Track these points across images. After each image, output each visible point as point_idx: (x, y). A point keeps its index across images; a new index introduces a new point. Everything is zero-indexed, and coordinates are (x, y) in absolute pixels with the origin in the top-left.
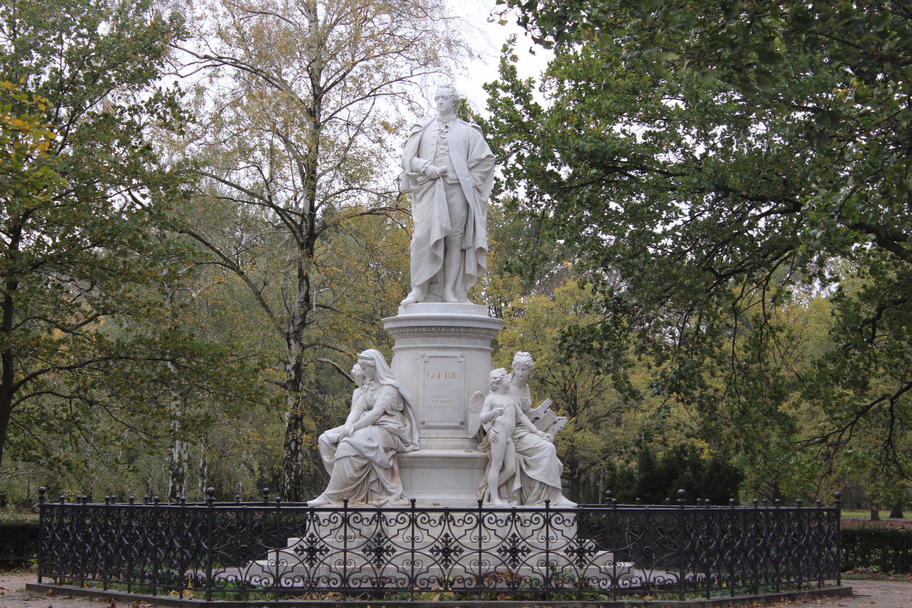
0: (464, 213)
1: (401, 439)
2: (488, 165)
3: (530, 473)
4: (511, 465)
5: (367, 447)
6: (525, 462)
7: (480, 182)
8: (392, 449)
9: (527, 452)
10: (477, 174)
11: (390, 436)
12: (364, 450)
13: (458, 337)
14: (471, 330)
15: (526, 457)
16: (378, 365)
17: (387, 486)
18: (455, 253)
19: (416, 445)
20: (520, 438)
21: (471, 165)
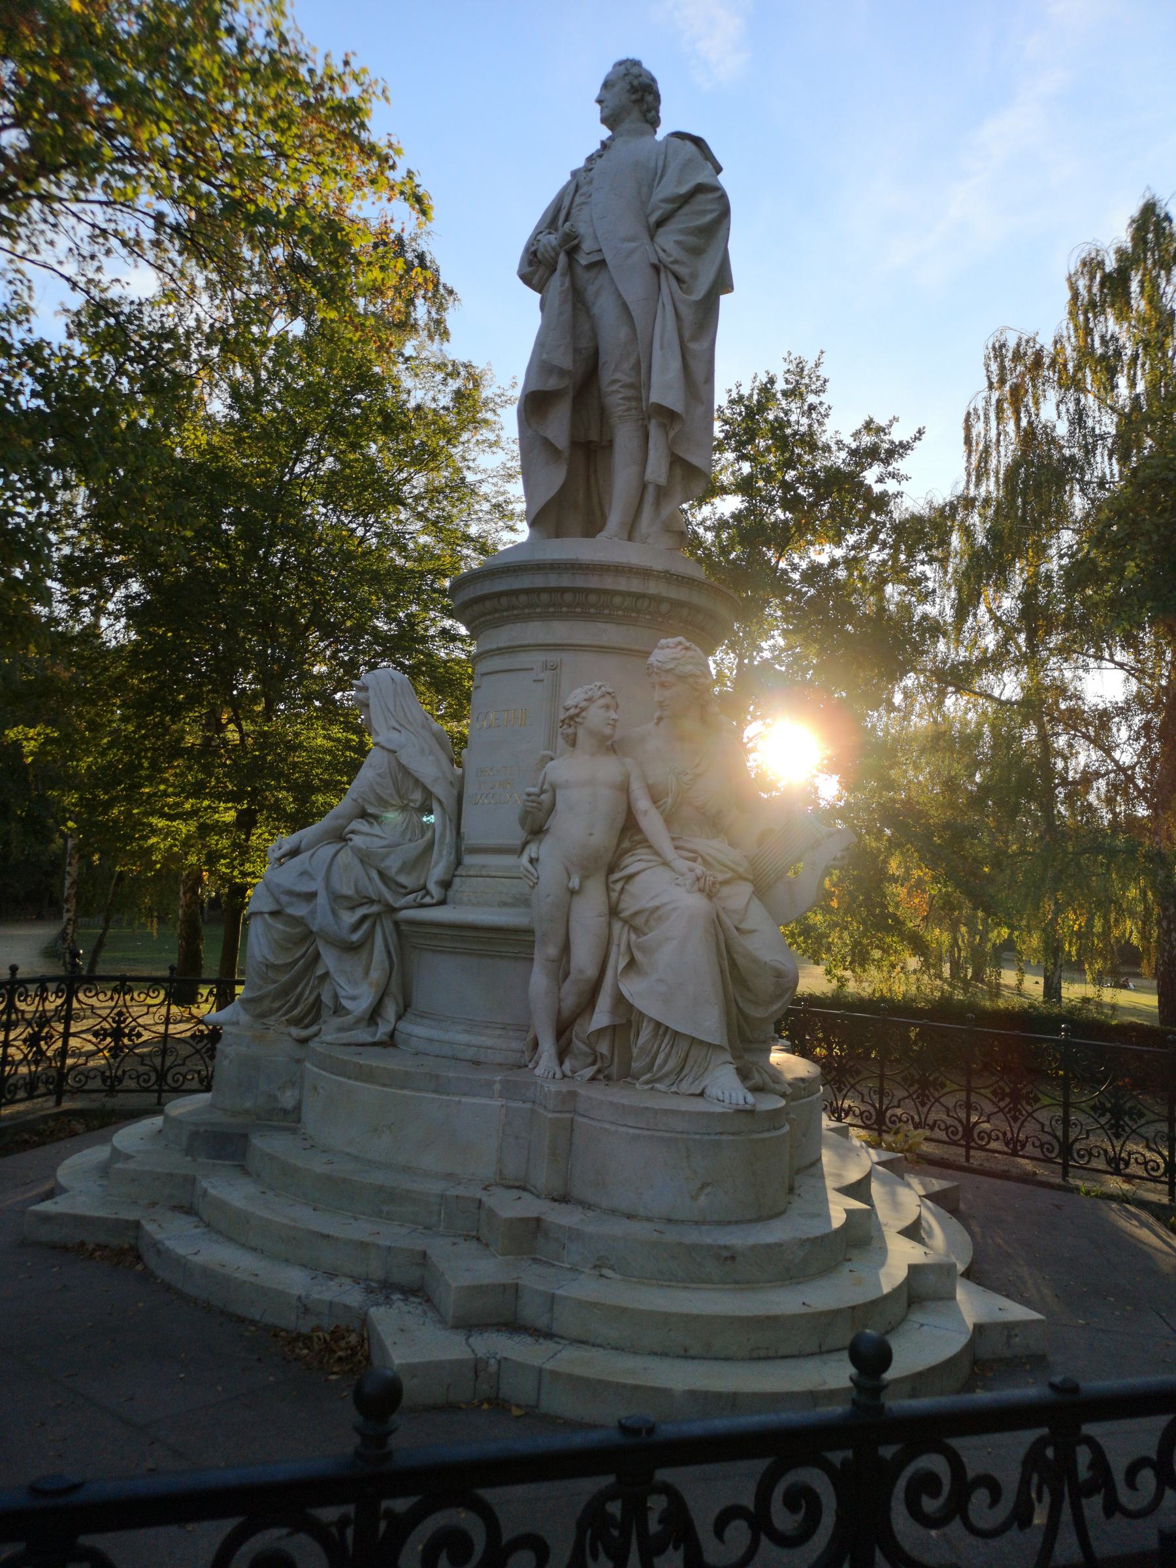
0: (623, 333)
1: (381, 874)
2: (705, 212)
3: (632, 988)
4: (583, 958)
5: (291, 893)
6: (629, 947)
7: (676, 253)
8: (371, 902)
9: (639, 921)
10: (669, 240)
11: (358, 868)
12: (285, 899)
13: (542, 617)
14: (568, 597)
15: (633, 937)
16: (371, 702)
17: (341, 993)
18: (625, 438)
19: (428, 893)
20: (630, 877)
21: (653, 219)
